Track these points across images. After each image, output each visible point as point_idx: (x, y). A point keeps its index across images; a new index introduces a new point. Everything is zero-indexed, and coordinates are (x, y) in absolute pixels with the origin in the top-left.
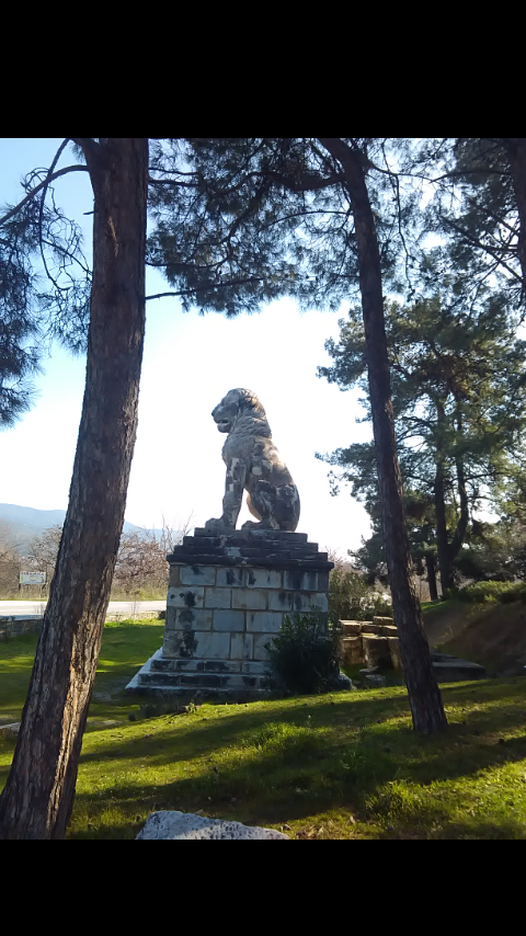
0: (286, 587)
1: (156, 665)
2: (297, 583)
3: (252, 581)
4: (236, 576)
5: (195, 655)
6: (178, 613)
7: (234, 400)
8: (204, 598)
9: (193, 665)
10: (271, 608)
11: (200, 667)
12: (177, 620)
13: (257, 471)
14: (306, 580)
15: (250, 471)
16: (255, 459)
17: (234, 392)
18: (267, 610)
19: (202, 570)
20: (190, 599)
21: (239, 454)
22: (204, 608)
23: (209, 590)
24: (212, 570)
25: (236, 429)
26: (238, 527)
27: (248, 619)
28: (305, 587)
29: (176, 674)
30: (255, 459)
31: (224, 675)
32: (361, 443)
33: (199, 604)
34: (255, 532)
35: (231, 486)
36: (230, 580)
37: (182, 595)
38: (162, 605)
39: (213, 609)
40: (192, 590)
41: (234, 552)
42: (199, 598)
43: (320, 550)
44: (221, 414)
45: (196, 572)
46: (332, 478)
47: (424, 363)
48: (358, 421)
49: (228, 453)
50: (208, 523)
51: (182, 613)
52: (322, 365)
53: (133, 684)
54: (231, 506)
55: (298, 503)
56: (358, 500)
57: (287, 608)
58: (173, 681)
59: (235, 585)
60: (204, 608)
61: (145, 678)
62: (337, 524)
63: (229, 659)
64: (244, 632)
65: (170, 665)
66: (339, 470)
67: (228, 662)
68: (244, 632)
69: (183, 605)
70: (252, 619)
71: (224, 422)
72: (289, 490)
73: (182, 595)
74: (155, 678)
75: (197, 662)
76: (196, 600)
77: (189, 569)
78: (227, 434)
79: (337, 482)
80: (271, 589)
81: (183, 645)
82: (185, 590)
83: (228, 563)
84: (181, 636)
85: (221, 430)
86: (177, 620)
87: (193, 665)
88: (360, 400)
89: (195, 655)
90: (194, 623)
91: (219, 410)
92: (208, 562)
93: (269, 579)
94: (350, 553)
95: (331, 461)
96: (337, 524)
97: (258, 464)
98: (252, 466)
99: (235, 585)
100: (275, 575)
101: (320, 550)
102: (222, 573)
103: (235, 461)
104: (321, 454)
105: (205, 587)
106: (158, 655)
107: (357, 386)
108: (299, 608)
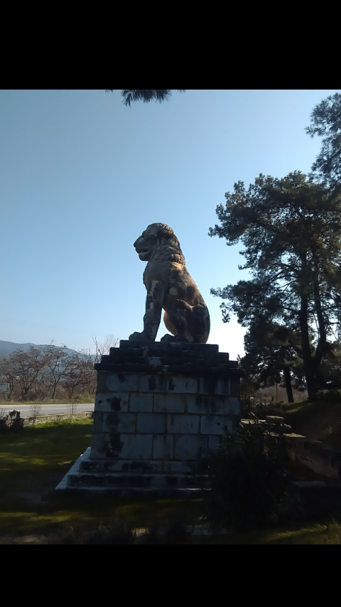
0: (202, 392)
1: (85, 466)
3: (172, 387)
4: (157, 382)
5: (121, 455)
6: (105, 417)
7: (153, 232)
8: (129, 402)
9: (119, 465)
10: (190, 410)
11: (125, 467)
12: (104, 423)
13: (173, 291)
14: (220, 385)
15: (167, 291)
16: (172, 281)
17: (154, 225)
18: (186, 413)
20: (116, 404)
21: (158, 278)
22: (129, 412)
25: (155, 257)
26: (158, 339)
28: (219, 391)
29: (102, 475)
30: (172, 281)
31: (147, 475)
32: (246, 281)
33: (124, 408)
34: (173, 344)
35: (152, 304)
36: (152, 386)
37: (108, 400)
38: (91, 407)
39: (137, 413)
40: (118, 396)
41: (155, 361)
42: (125, 403)
43: (230, 359)
44: (141, 244)
45: (122, 379)
46: (223, 309)
47: (290, 224)
48: (240, 268)
49: (148, 278)
50: (131, 337)
51: (107, 416)
52: (217, 224)
53: (62, 485)
54: (151, 322)
55: (208, 319)
56: (244, 325)
57: (203, 412)
58: (99, 482)
59: (156, 391)
60: (129, 412)
61: (73, 479)
62: (229, 337)
63: (152, 459)
64: (165, 433)
65: (98, 466)
66: (227, 301)
67: (152, 462)
68: (165, 433)
69: (110, 410)
70: (172, 422)
71: (145, 251)
72: (200, 308)
73: (108, 400)
74: (83, 478)
75: (121, 463)
76: (121, 404)
78: (147, 262)
79: (227, 311)
80: (189, 394)
81: (110, 446)
84: (108, 438)
85: (142, 258)
86: (104, 423)
87: (119, 465)
88: (241, 253)
89: (121, 455)
91: (140, 241)
93: (187, 385)
95: (223, 296)
96: (229, 337)
97: (176, 285)
98: (169, 288)
99: (156, 391)
100: (191, 381)
101: (230, 359)
103: (155, 283)
104: (216, 290)
106: (84, 457)
107: (240, 241)
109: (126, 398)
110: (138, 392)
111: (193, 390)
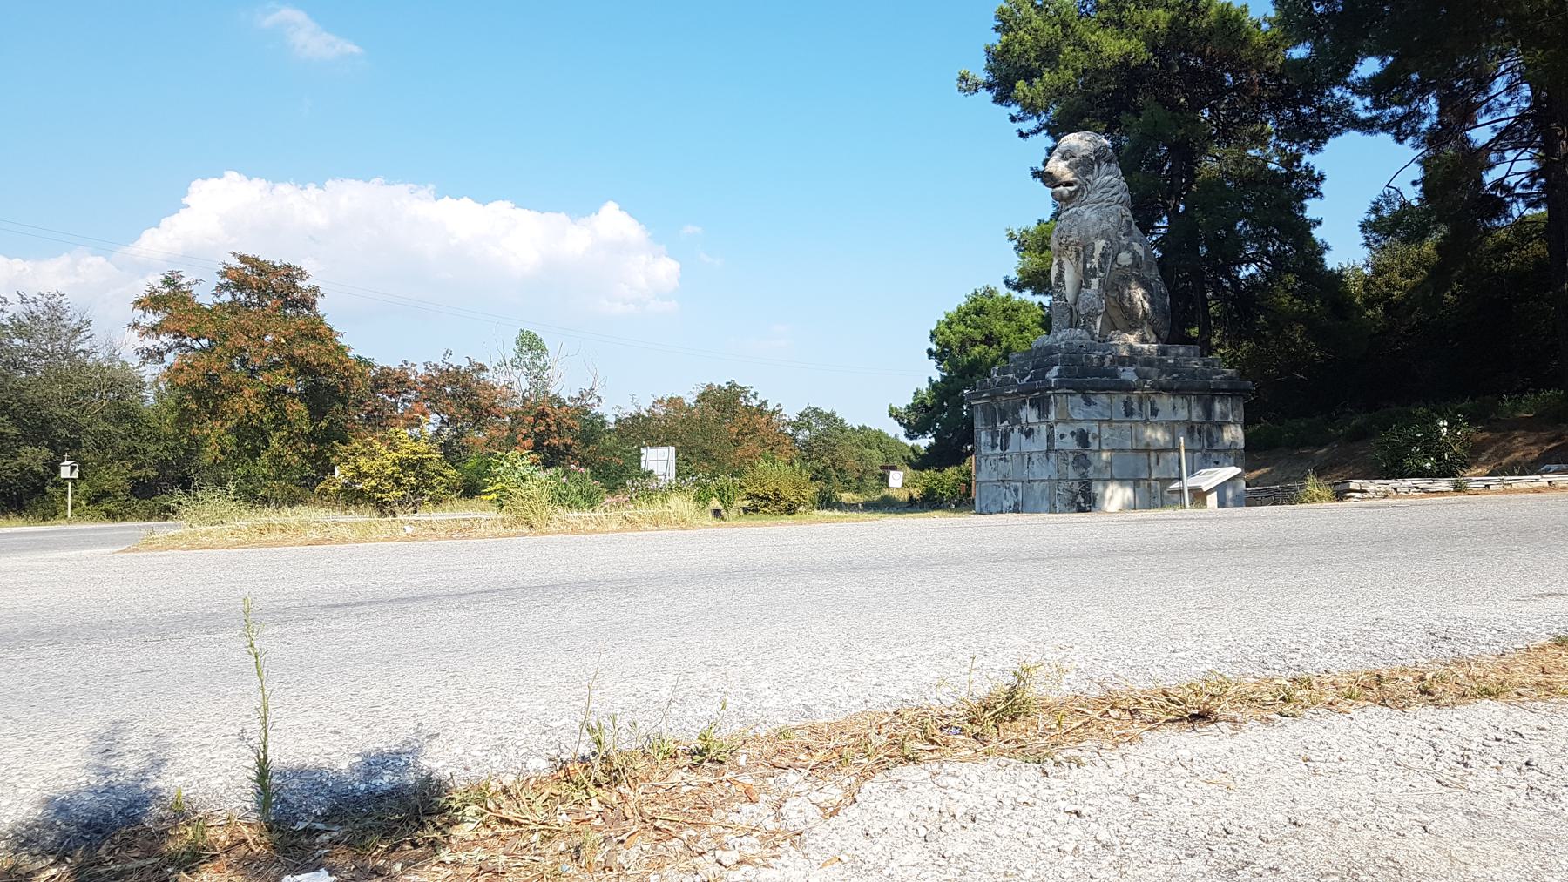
0: (1194, 418)
2: (1208, 411)
3: (1155, 412)
4: (1135, 406)
6: (1071, 459)
14: (1218, 407)
19: (1093, 398)
20: (1082, 438)
23: (1104, 425)
24: (1104, 398)
27: (1153, 459)
36: (1129, 412)
37: (1073, 434)
40: (1084, 426)
41: (1128, 374)
42: (1094, 438)
45: (1088, 403)
57: (1198, 447)
59: (1135, 418)
73: (1073, 434)
77: (1078, 398)
82: (1076, 427)
83: (1126, 388)
84: (1076, 488)
90: (1091, 469)
92: (1103, 389)
94: (894, 414)
99: (1135, 418)
102: (1119, 400)
105: (1101, 421)
108: (1210, 445)
109: (1096, 431)
110: (1109, 421)
111: (1183, 414)
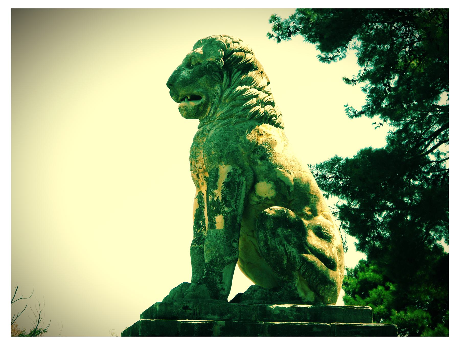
44: (186, 83)
71: (195, 98)
78: (196, 122)
85: (188, 114)
98: (256, 181)
